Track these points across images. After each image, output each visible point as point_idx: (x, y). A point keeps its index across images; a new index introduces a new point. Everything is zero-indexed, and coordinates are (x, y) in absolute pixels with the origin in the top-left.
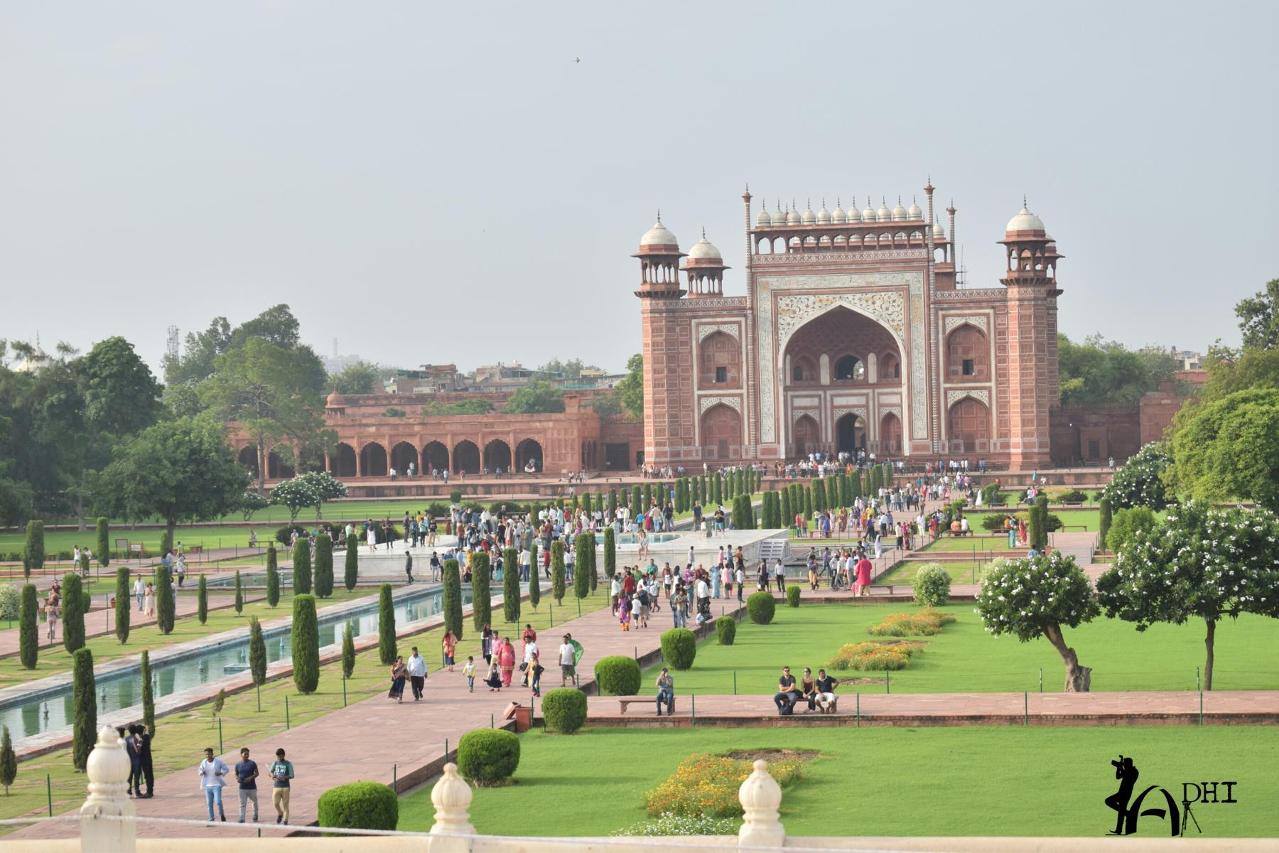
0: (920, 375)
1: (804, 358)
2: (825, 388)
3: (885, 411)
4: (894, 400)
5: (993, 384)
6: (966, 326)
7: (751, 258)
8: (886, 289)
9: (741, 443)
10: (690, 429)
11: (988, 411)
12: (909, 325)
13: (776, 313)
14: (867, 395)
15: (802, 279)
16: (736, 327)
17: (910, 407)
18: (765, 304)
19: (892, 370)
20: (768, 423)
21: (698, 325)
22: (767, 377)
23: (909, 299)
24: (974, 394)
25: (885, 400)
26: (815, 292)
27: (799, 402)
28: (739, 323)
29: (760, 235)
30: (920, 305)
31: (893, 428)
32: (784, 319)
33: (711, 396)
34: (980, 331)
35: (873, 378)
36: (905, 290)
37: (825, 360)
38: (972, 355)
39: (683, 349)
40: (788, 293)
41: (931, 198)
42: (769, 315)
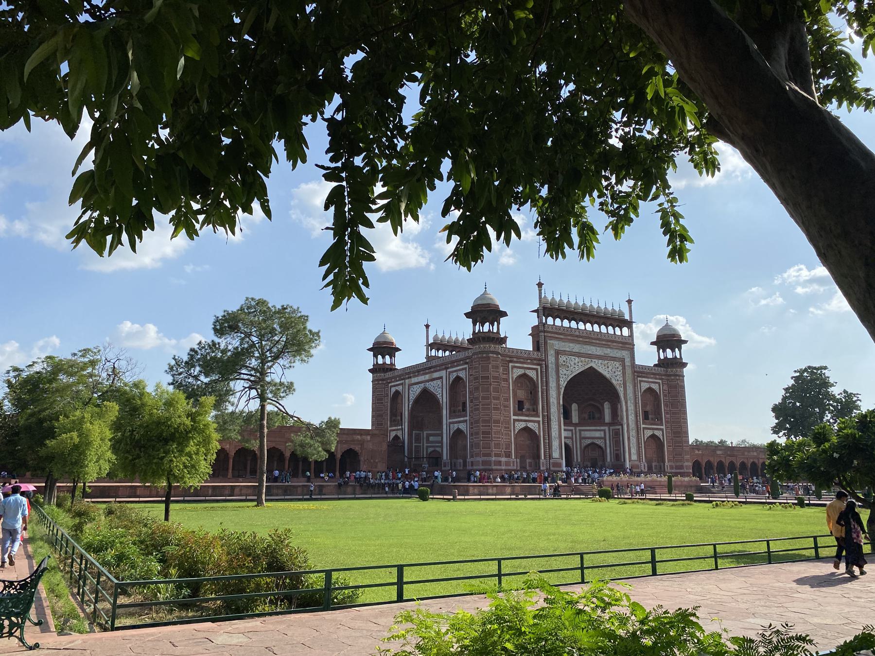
0: (632, 417)
3: (589, 441)
5: (664, 427)
8: (614, 359)
9: (539, 457)
10: (508, 446)
14: (571, 430)
15: (571, 345)
16: (534, 372)
17: (629, 438)
18: (551, 359)
20: (555, 444)
21: (513, 367)
26: (579, 355)
28: (536, 370)
30: (629, 371)
32: (562, 371)
33: (521, 421)
36: (622, 361)
38: (648, 408)
39: (503, 384)
40: (564, 353)
41: (630, 308)
42: (554, 366)
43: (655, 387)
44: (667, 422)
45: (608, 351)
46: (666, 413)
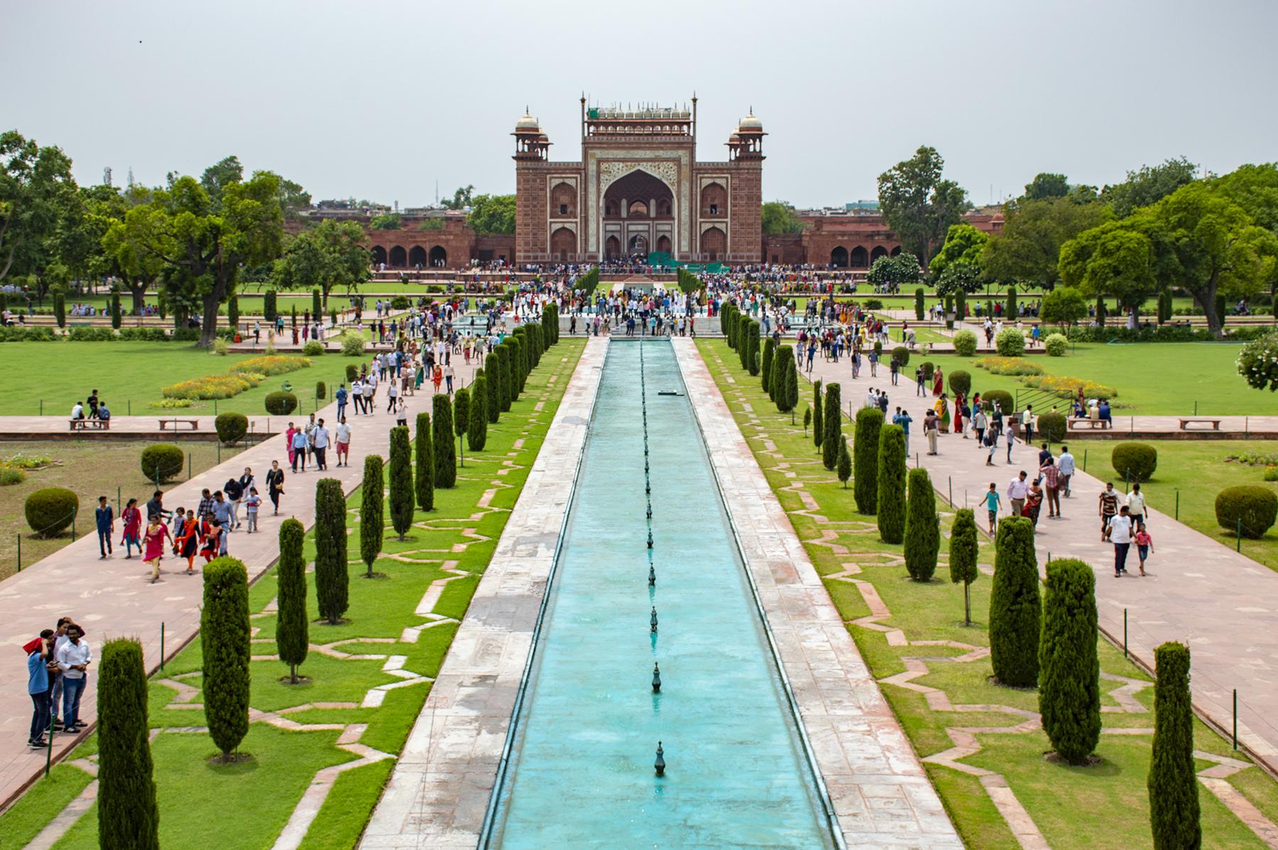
0: (685, 213)
1: (613, 202)
2: (624, 219)
4: (667, 228)
6: (714, 184)
7: (584, 138)
8: (667, 160)
9: (575, 251)
10: (544, 242)
11: (725, 236)
12: (679, 182)
13: (599, 173)
18: (592, 168)
19: (664, 210)
20: (592, 240)
22: (592, 212)
23: (679, 166)
24: (718, 226)
25: (660, 228)
26: (623, 160)
27: (610, 228)
29: (590, 124)
30: (686, 170)
31: (665, 245)
34: (722, 187)
35: (653, 214)
36: (677, 161)
37: (624, 202)
38: (716, 202)
39: (541, 193)
40: (607, 160)
43: (721, 182)
44: (733, 214)
45: (661, 153)
46: (733, 205)
